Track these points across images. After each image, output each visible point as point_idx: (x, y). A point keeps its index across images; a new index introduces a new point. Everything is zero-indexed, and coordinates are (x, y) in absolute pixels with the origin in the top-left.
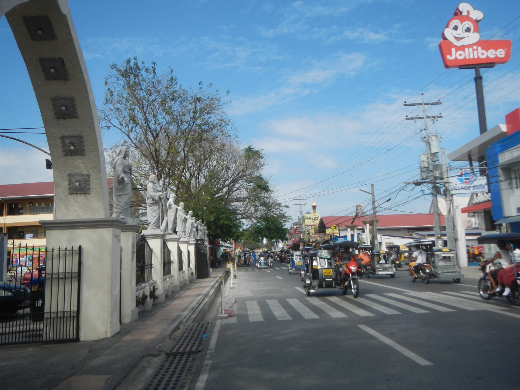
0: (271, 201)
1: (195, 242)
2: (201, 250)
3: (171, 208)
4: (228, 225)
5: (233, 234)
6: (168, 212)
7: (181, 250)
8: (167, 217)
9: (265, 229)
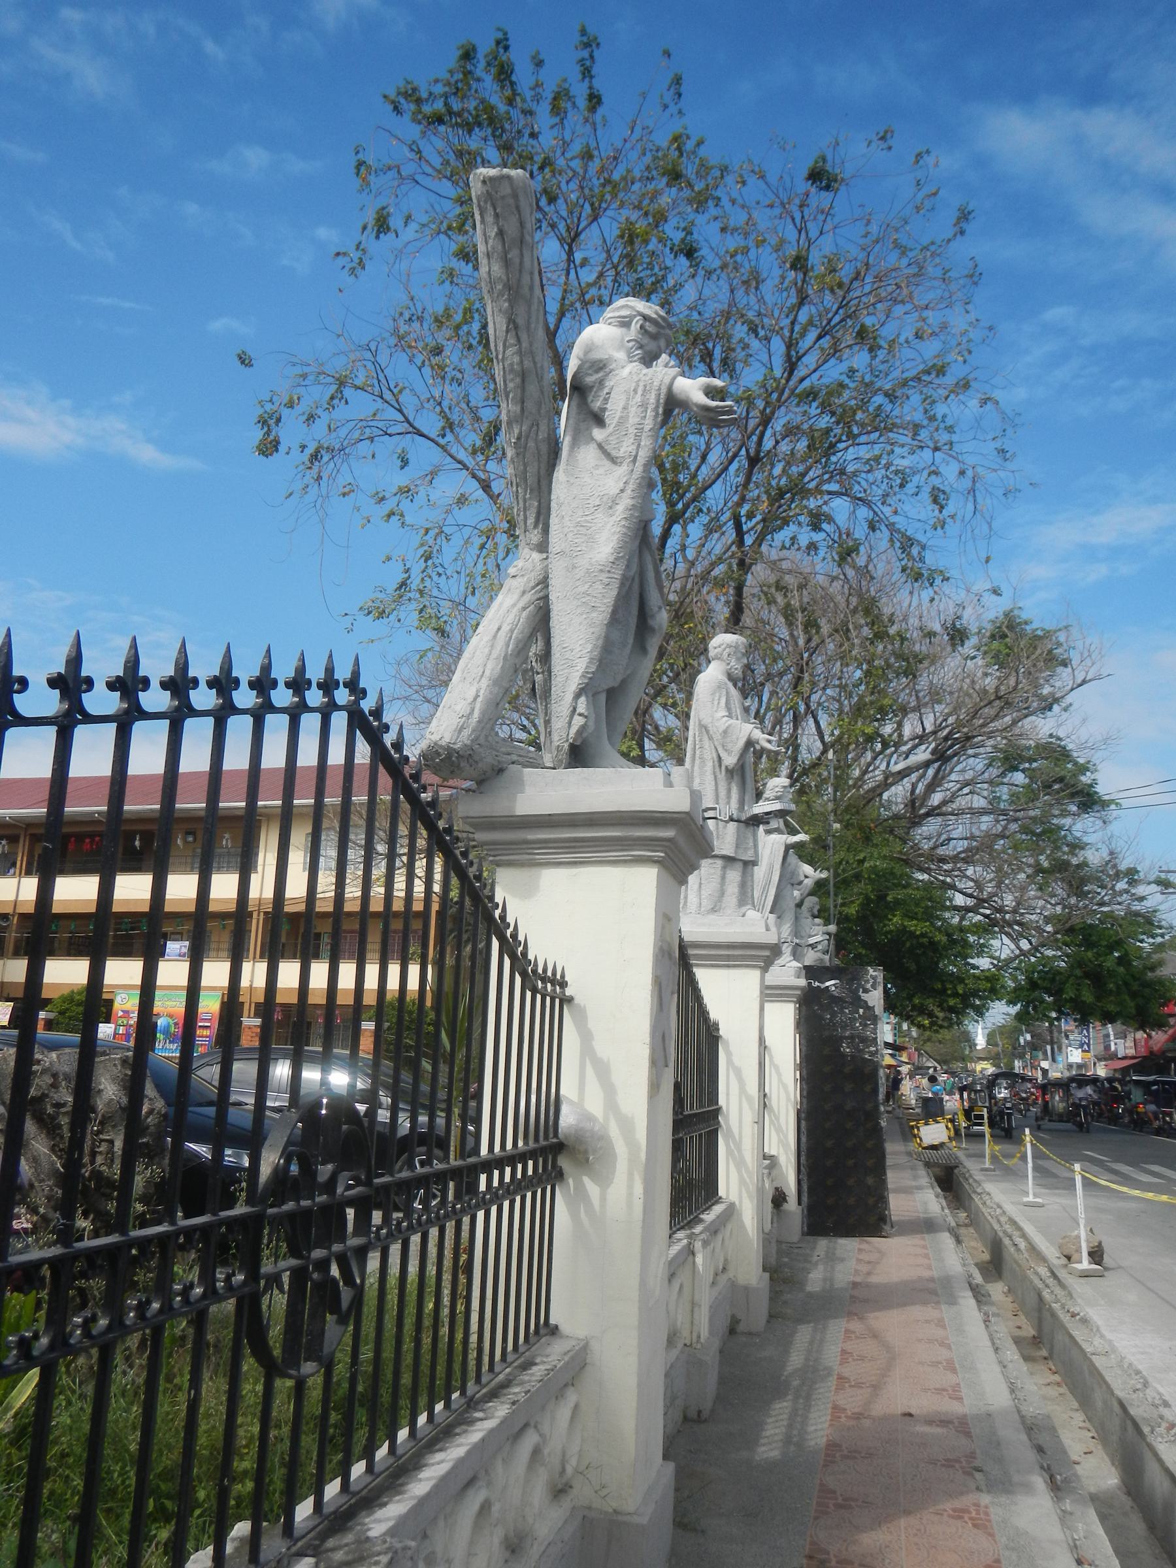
0: (1094, 857)
1: (802, 982)
2: (841, 1039)
3: (598, 420)
4: (925, 940)
5: (949, 986)
6: (560, 475)
7: (713, 1016)
8: (543, 547)
9: (1078, 972)
